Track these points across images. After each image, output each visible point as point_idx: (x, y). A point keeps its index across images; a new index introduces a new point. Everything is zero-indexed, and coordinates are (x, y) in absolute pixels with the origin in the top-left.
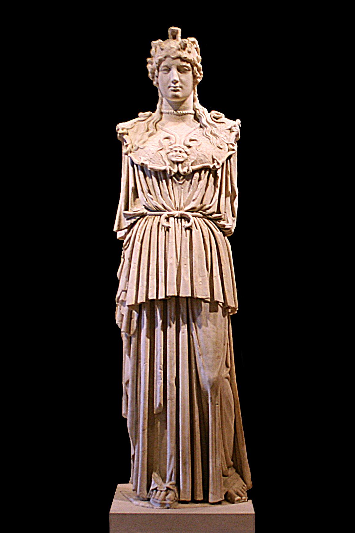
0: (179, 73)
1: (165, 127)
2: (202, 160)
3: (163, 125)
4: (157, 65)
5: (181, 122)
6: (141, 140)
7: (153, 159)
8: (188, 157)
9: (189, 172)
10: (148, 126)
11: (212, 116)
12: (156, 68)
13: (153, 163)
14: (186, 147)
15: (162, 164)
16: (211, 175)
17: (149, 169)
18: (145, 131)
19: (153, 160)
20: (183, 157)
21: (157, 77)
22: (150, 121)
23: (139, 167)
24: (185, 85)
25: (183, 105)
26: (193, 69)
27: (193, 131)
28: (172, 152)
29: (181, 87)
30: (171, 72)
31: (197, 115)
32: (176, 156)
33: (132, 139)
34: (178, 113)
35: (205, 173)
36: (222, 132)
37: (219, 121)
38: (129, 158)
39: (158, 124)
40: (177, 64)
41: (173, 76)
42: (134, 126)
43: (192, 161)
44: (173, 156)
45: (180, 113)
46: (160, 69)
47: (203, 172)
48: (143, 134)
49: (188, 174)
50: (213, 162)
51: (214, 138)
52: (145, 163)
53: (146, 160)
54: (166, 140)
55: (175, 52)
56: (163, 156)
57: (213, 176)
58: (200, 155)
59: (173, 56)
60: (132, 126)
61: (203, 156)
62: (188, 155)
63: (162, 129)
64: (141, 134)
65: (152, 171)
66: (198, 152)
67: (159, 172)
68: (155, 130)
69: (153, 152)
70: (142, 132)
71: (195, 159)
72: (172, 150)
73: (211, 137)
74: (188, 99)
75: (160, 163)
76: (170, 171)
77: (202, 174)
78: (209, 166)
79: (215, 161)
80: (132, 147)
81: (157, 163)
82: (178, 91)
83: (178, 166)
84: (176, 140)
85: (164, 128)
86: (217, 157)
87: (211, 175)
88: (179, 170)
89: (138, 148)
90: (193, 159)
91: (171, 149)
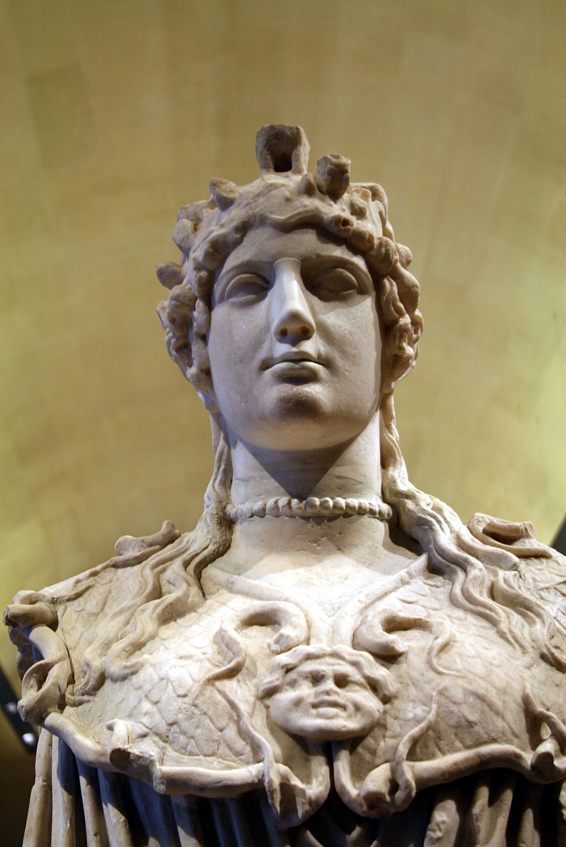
0: (315, 300)
1: (249, 577)
2: (471, 724)
3: (239, 570)
4: (204, 274)
5: (329, 553)
6: (117, 639)
7: (185, 725)
8: (385, 712)
9: (400, 795)
10: (158, 577)
11: (480, 529)
12: (195, 291)
13: (184, 750)
14: (366, 658)
15: (238, 754)
16: (529, 817)
17: (160, 788)
18: (138, 600)
19: (184, 733)
20: (358, 708)
21: (204, 338)
22: (171, 559)
23: (103, 783)
24: (344, 354)
25: (337, 470)
26: (379, 288)
27: (396, 589)
28: (293, 684)
29: (326, 362)
30: (272, 294)
31: (404, 518)
32: (315, 706)
33: (69, 645)
34: (313, 506)
35: (493, 800)
36: (543, 594)
37: (517, 546)
38: (55, 739)
39: (211, 571)
40: (302, 250)
41: (283, 300)
42: (88, 588)
43: (415, 730)
44: (298, 703)
45: (324, 505)
46: (218, 289)
47: (484, 794)
48: (132, 611)
49: (392, 810)
50: (536, 741)
51: (516, 618)
52: (135, 750)
53: (144, 736)
54: (255, 630)
55: (288, 200)
56: (244, 708)
57: (538, 825)
58: (458, 695)
59: (280, 217)
60: (80, 588)
61: (471, 699)
62: (386, 700)
63: (231, 590)
64: (120, 612)
65: (178, 800)
66: (445, 682)
67: (221, 803)
68: (195, 590)
69: (181, 692)
70: (127, 603)
71: (431, 717)
72: (293, 675)
73: (503, 614)
74: (361, 441)
75: (223, 749)
76: (286, 788)
77: (476, 810)
78: (518, 757)
79: (546, 732)
80: (71, 681)
81: (208, 749)
82: (313, 378)
83: (330, 764)
84: (309, 627)
85: (242, 581)
86: (548, 709)
87: (529, 817)
88: (338, 788)
89: (102, 679)
90: (418, 721)
91: (288, 669)
